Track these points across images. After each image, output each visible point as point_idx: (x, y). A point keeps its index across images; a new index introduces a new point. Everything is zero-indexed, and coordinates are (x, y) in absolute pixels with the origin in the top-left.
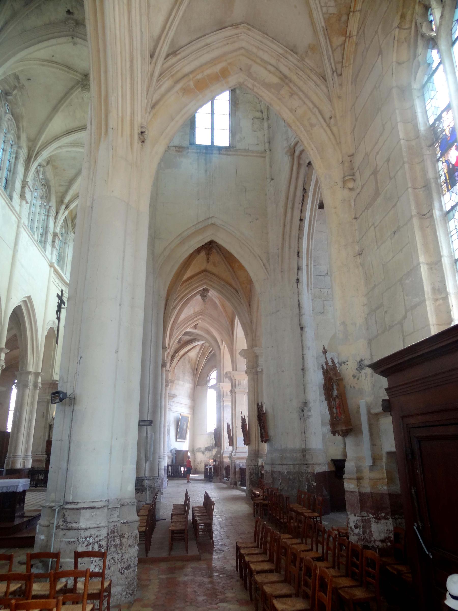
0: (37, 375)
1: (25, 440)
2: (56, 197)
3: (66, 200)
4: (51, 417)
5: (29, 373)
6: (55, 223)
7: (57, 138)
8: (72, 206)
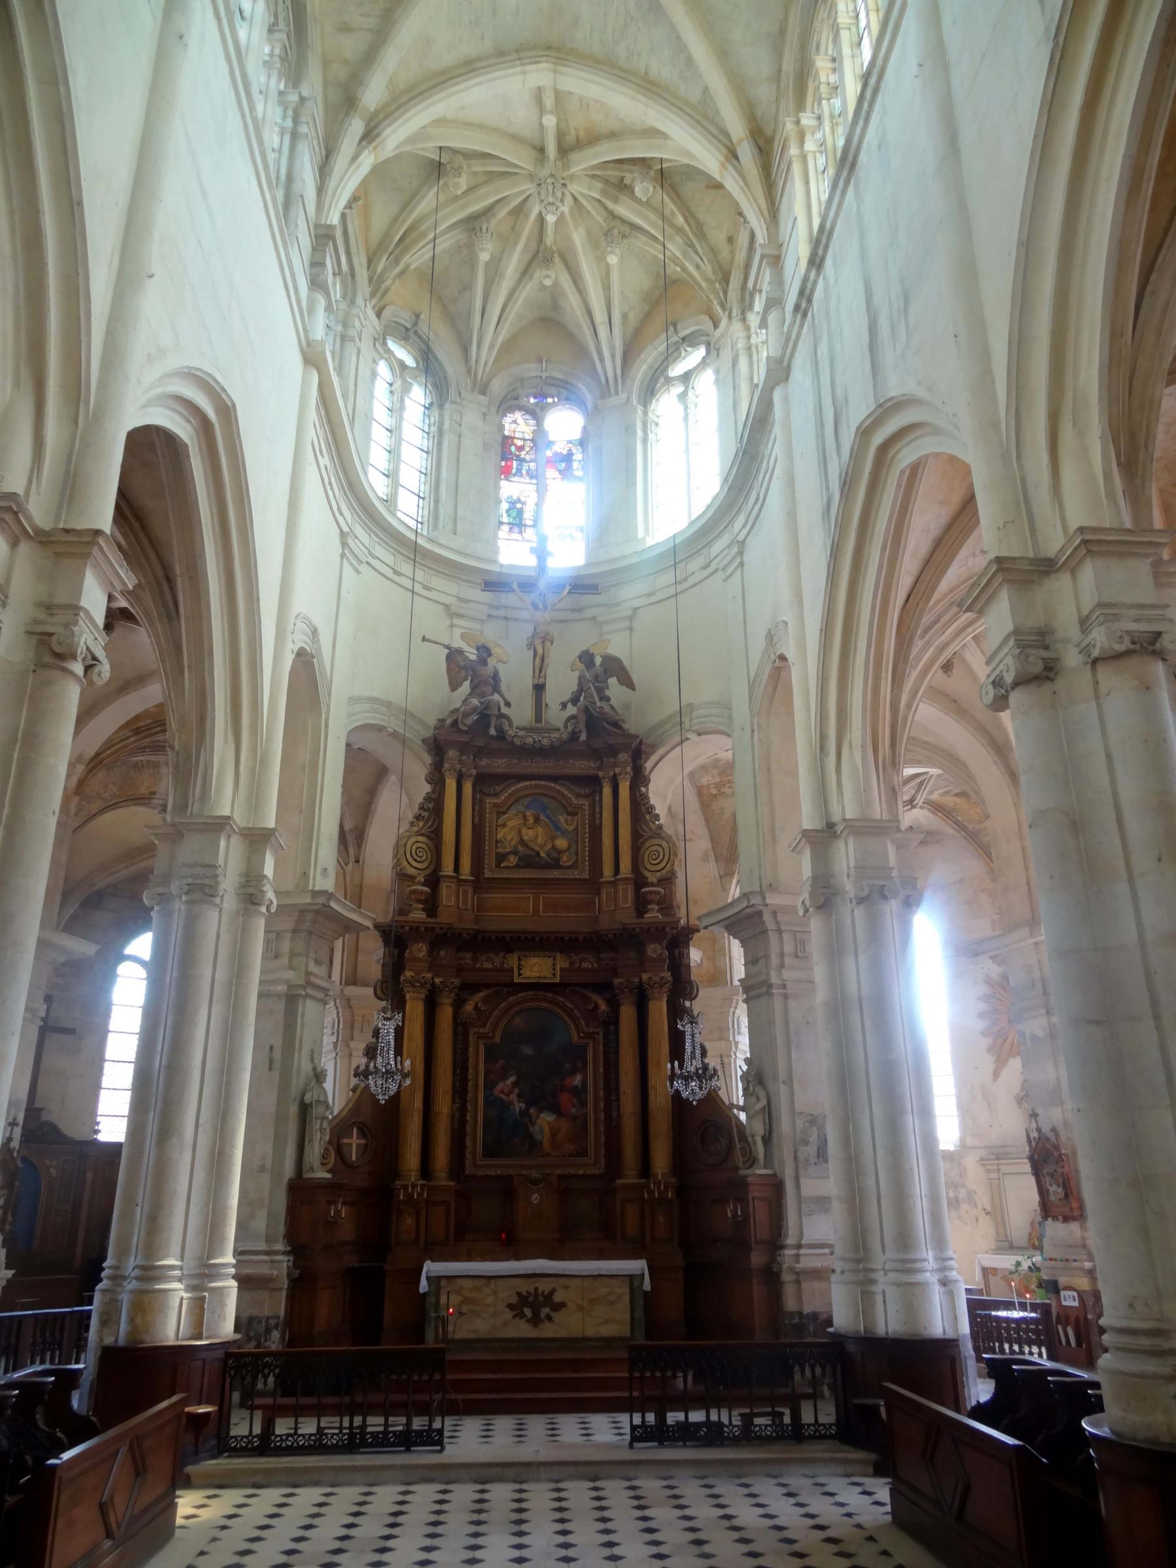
0: (257, 839)
1: (200, 1176)
2: (326, 83)
4: (306, 1067)
5: (220, 825)
6: (320, 190)
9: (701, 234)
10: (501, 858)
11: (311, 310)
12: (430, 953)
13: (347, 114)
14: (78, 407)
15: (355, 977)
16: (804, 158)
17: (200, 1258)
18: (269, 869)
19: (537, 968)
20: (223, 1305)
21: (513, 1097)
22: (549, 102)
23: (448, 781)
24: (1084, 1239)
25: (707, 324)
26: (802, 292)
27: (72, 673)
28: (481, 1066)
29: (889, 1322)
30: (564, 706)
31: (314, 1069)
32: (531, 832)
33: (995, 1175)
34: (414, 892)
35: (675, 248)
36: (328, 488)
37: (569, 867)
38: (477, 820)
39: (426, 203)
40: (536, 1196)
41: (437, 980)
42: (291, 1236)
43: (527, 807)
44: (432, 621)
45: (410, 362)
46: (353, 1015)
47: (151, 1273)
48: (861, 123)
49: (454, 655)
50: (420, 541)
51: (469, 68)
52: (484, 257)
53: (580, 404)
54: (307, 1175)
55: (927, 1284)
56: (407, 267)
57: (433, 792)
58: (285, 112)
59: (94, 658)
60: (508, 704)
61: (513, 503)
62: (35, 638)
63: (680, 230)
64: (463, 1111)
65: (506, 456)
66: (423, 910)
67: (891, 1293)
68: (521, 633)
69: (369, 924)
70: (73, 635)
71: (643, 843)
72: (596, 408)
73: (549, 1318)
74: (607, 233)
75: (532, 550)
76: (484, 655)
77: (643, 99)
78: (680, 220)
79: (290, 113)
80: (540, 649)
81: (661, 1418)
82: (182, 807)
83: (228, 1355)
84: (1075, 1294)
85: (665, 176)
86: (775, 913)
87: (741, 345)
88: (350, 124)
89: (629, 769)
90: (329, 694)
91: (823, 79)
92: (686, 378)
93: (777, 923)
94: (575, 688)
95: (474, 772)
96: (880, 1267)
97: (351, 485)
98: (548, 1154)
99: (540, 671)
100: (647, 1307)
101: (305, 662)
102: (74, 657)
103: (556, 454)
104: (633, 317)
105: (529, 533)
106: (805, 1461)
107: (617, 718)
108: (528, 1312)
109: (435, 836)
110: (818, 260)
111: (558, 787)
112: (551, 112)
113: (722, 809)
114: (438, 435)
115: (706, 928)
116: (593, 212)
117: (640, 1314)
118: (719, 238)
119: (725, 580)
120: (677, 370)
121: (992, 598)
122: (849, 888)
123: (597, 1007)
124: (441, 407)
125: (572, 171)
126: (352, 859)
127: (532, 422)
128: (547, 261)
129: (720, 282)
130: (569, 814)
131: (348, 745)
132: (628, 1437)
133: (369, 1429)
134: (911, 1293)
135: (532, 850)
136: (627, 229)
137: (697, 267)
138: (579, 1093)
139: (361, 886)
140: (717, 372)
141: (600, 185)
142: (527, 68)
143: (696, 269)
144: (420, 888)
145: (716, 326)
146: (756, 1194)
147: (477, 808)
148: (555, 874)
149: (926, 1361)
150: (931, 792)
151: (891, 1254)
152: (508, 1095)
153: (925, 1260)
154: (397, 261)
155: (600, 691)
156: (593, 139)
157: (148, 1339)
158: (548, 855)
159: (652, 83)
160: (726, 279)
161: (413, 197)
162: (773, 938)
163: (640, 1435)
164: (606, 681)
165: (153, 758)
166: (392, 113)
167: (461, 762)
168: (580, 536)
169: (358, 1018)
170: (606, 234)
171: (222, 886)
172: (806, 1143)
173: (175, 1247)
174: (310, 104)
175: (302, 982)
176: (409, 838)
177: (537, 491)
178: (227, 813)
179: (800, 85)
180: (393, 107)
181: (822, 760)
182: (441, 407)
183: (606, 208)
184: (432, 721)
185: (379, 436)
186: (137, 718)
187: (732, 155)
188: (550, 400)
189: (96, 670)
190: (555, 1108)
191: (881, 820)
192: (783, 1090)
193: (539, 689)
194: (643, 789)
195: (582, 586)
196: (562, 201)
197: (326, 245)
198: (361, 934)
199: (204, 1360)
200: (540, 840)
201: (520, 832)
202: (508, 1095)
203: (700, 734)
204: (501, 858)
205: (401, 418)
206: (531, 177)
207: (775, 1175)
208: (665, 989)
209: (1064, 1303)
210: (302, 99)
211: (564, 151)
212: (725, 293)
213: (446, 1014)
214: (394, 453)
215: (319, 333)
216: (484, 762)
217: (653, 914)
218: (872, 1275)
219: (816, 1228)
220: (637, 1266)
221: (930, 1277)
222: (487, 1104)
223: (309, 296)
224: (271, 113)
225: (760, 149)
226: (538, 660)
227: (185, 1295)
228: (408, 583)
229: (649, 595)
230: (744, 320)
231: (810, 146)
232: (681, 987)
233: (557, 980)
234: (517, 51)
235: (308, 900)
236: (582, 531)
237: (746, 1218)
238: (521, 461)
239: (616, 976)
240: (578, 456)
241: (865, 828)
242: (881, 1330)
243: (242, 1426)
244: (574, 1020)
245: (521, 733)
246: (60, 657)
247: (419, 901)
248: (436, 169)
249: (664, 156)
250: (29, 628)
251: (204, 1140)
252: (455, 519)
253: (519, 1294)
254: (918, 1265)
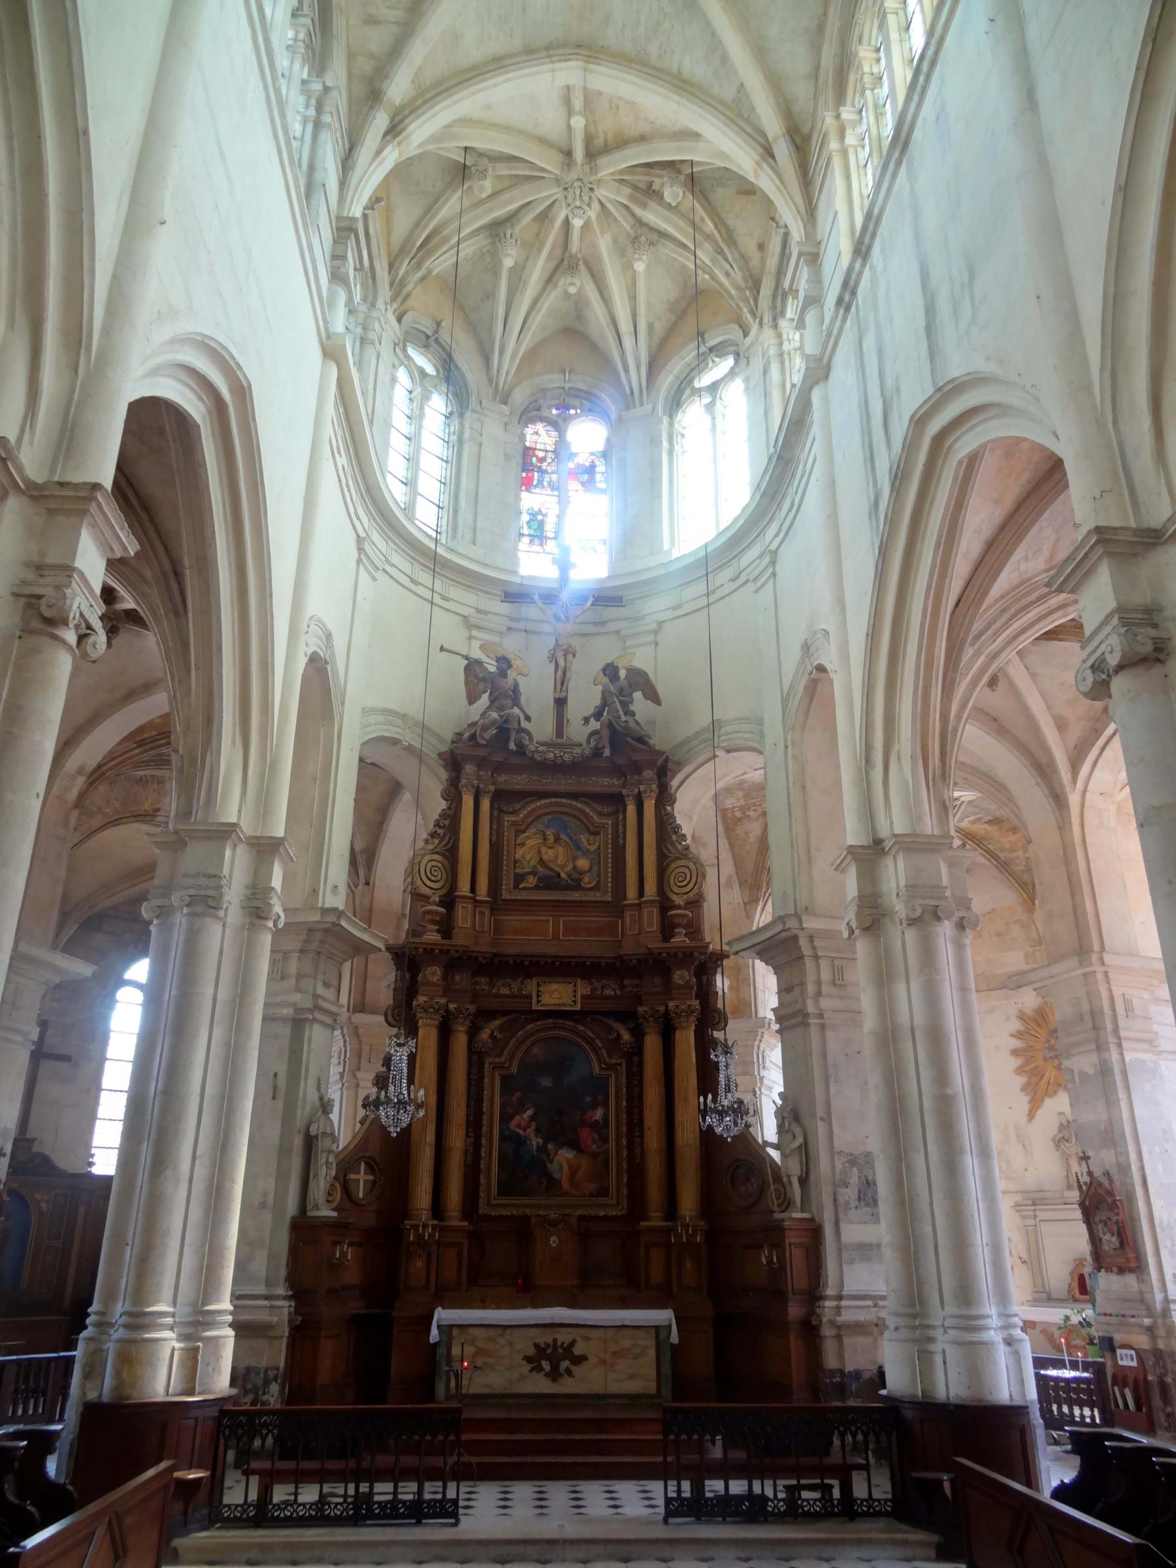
0: (265, 849)
2: (350, 76)
4: (312, 1095)
5: (227, 832)
6: (343, 183)
9: (732, 242)
10: (519, 878)
11: (331, 304)
12: (444, 977)
13: (372, 107)
14: (78, 354)
15: (363, 1003)
16: (844, 152)
17: (194, 1304)
18: (277, 882)
19: (557, 994)
20: (218, 1358)
21: (530, 1131)
22: (578, 103)
23: (464, 797)
24: (1141, 1292)
25: (735, 333)
26: (845, 284)
27: (63, 642)
28: (497, 1100)
29: (949, 1385)
30: (586, 720)
31: (321, 1099)
32: (551, 852)
33: (1030, 1222)
34: (428, 912)
35: (704, 257)
36: (346, 489)
37: (590, 889)
38: (494, 839)
39: (450, 206)
40: (553, 1238)
41: (452, 1006)
42: (293, 1280)
43: (547, 826)
44: (450, 632)
45: (430, 370)
46: (360, 1043)
47: (140, 1321)
48: (916, 98)
49: (472, 667)
50: (440, 551)
51: (497, 64)
52: (508, 263)
53: (604, 415)
54: (312, 1213)
55: (993, 1343)
56: (430, 272)
57: (449, 808)
58: (308, 101)
59: (89, 627)
60: (528, 718)
61: (533, 515)
62: (23, 600)
63: (708, 237)
64: (477, 1145)
65: (528, 468)
66: (438, 931)
67: (952, 1353)
68: (542, 647)
69: (381, 945)
70: (65, 598)
71: (668, 865)
72: (620, 418)
73: (569, 1372)
74: (635, 240)
75: (554, 561)
76: (505, 666)
77: (675, 97)
78: (709, 226)
79: (313, 102)
80: (562, 660)
81: (698, 1489)
82: (186, 813)
83: (223, 1413)
84: (1133, 1352)
85: (695, 181)
86: (811, 938)
87: (772, 351)
88: (375, 118)
89: (654, 787)
90: (343, 704)
91: (866, 69)
92: (714, 388)
93: (814, 948)
94: (597, 701)
95: (492, 788)
96: (939, 1323)
97: (368, 490)
98: (567, 1194)
99: (562, 685)
100: (674, 1360)
101: (318, 671)
102: (65, 622)
103: (579, 466)
104: (660, 328)
105: (551, 545)
106: (860, 1542)
107: (643, 733)
108: (546, 1365)
109: (451, 854)
110: (864, 249)
111: (579, 805)
112: (580, 113)
113: (746, 833)
114: (458, 444)
115: (736, 953)
116: (621, 219)
117: (666, 1369)
118: (749, 245)
119: (756, 592)
120: (705, 380)
121: (1088, 574)
122: (900, 908)
123: (619, 1037)
124: (461, 416)
125: (599, 175)
126: (362, 881)
127: (554, 434)
128: (572, 269)
129: (750, 290)
130: (591, 833)
131: (361, 760)
132: (661, 1510)
133: (377, 1498)
134: (974, 1354)
135: (552, 870)
136: (655, 237)
137: (727, 274)
138: (600, 1128)
139: (371, 910)
140: (747, 380)
141: (628, 190)
142: (557, 65)
143: (726, 277)
144: (434, 908)
145: (745, 335)
146: (793, 1240)
147: (495, 827)
148: (576, 896)
149: (989, 1431)
150: (961, 820)
151: (950, 1309)
152: (525, 1130)
153: (989, 1316)
154: (419, 266)
155: (624, 705)
156: (622, 142)
157: (135, 1395)
158: (569, 876)
159: (685, 82)
160: (756, 286)
161: (436, 201)
162: (809, 964)
163: (675, 1509)
164: (631, 695)
165: (158, 773)
166: (419, 107)
167: (478, 777)
168: (602, 549)
169: (366, 1048)
170: (633, 242)
171: (226, 898)
172: (846, 1185)
173: (167, 1291)
174: (334, 93)
175: (309, 1005)
176: (424, 855)
177: (559, 503)
178: (235, 821)
179: (841, 78)
180: (419, 102)
181: (867, 773)
182: (461, 416)
183: (633, 215)
184: (449, 736)
185: (398, 443)
186: (141, 729)
187: (768, 153)
188: (572, 412)
189: (91, 640)
190: (575, 1145)
191: (933, 836)
192: (821, 1127)
193: (561, 703)
194: (669, 808)
195: (606, 599)
196: (589, 205)
197: (348, 238)
198: (372, 956)
199: (197, 1419)
200: (560, 860)
201: (539, 852)
202: (525, 1130)
203: (728, 752)
204: (519, 878)
205: (420, 427)
206: (557, 181)
207: (812, 1219)
208: (692, 1019)
209: (1120, 1363)
210: (326, 89)
211: (592, 155)
212: (756, 300)
213: (460, 1041)
214: (412, 461)
215: (339, 326)
216: (503, 778)
217: (680, 939)
218: (931, 1333)
219: (862, 1277)
220: (664, 1316)
221: (994, 1336)
222: (502, 1138)
223: (329, 289)
224: (296, 100)
225: (797, 147)
226: (560, 673)
227: (177, 1345)
228: (427, 594)
229: (674, 608)
230: (776, 326)
231: (850, 140)
232: (710, 1016)
233: (578, 1007)
234: (547, 49)
235: (317, 918)
236: (604, 543)
237: (782, 1267)
238: (543, 472)
239: (641, 1004)
240: (600, 468)
241: (913, 844)
242: (941, 1393)
243: (238, 1492)
244: (595, 1050)
245: (541, 748)
246: (50, 622)
247: (433, 922)
248: (461, 172)
249: (696, 159)
250: (16, 590)
251: (201, 1173)
252: (475, 529)
253: (537, 1346)
254: (981, 1322)
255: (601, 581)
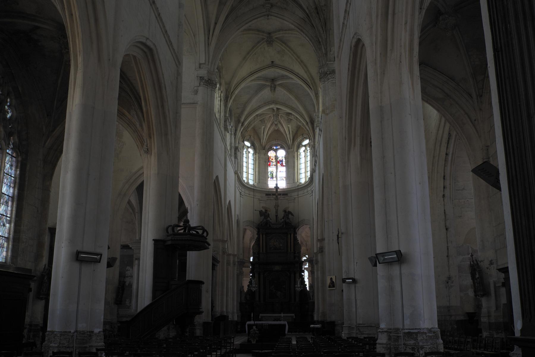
3: (242, 120)
6: (235, 138)
7: (244, 79)
8: (246, 123)
49: (261, 212)
51: (259, 107)
80: (277, 206)
92: (305, 146)
105: (275, 179)
168: (284, 179)
185: (245, 164)
187: (307, 124)
193: (277, 216)
195: (285, 193)
255: (284, 189)
